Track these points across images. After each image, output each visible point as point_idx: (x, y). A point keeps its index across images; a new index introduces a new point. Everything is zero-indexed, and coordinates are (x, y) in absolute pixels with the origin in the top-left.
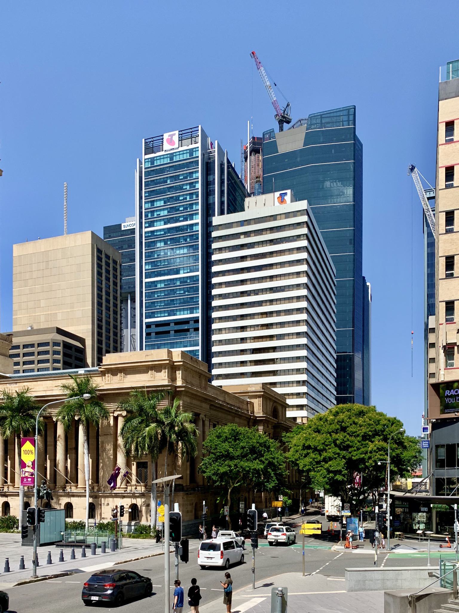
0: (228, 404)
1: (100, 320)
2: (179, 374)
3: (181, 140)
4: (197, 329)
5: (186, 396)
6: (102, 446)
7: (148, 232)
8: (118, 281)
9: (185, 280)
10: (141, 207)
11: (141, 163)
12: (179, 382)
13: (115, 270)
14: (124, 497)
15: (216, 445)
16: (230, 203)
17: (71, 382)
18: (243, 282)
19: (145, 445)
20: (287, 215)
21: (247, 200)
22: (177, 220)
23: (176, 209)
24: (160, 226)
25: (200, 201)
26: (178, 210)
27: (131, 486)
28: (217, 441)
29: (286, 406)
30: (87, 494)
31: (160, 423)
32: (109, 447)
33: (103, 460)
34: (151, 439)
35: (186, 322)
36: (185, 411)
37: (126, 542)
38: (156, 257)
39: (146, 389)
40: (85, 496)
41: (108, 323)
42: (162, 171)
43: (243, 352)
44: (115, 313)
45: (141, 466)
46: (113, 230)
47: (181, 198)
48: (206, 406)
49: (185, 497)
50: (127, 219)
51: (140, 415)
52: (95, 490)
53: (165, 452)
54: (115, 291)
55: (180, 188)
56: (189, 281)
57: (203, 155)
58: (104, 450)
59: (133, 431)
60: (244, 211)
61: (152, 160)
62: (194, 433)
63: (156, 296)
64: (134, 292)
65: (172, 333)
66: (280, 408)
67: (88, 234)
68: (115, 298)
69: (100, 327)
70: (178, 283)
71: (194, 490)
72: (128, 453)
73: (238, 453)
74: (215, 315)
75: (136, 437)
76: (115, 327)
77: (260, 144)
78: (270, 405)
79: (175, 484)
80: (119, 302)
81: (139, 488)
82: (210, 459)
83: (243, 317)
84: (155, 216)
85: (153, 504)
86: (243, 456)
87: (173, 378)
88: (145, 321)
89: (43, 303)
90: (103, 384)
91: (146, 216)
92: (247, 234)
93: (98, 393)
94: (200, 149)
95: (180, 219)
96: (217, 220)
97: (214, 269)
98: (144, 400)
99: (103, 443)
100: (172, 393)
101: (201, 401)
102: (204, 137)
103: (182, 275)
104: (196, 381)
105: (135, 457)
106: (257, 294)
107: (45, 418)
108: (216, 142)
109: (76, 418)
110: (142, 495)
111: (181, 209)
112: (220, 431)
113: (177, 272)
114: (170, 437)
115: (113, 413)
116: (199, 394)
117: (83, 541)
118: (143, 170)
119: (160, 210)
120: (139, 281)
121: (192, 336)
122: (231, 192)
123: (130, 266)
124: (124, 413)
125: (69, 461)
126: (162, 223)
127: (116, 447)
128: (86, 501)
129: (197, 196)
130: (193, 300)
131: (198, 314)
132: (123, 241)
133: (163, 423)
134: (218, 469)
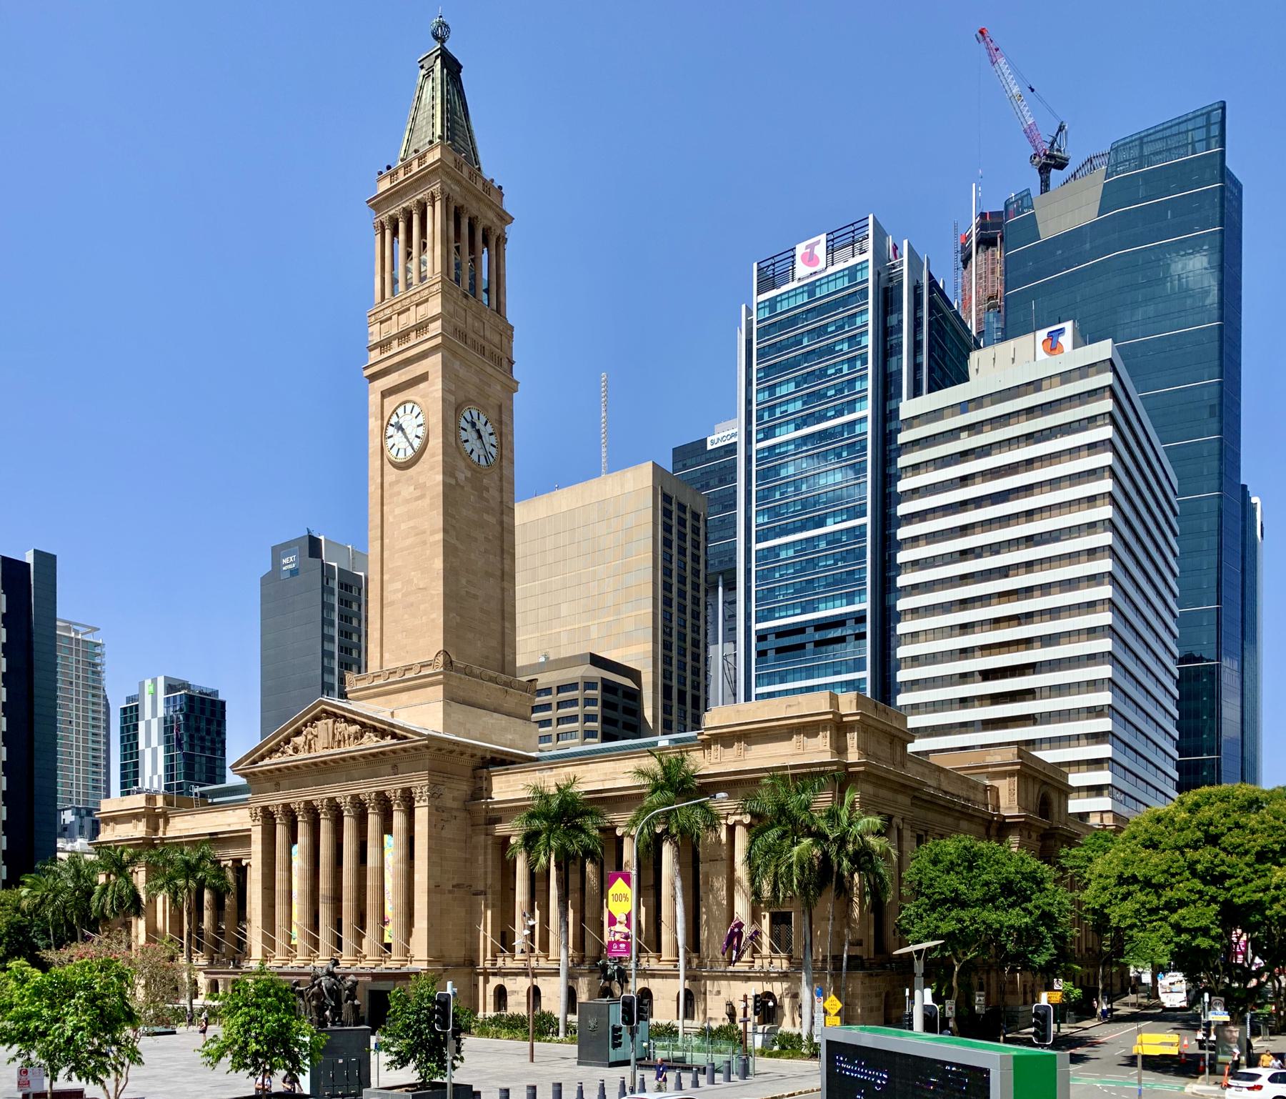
0: (946, 793)
1: (667, 632)
2: (852, 740)
3: (831, 250)
4: (863, 636)
5: (867, 781)
6: (707, 882)
7: (763, 450)
8: (702, 552)
9: (838, 536)
10: (749, 402)
11: (749, 312)
12: (853, 756)
13: (696, 531)
14: (748, 979)
15: (931, 879)
16: (933, 365)
17: (651, 764)
18: (964, 530)
19: (792, 881)
20: (1065, 377)
21: (974, 356)
22: (822, 418)
23: (820, 395)
24: (787, 434)
25: (870, 371)
26: (825, 396)
27: (761, 958)
28: (932, 872)
29: (1067, 791)
30: (682, 973)
31: (819, 837)
32: (720, 884)
33: (708, 907)
34: (802, 868)
35: (838, 622)
36: (866, 813)
37: (761, 1064)
38: (778, 497)
39: (789, 772)
40: (677, 977)
41: (682, 637)
42: (792, 321)
43: (964, 677)
44: (696, 615)
45: (780, 920)
46: (690, 453)
47: (831, 371)
48: (904, 800)
49: (867, 981)
50: (717, 427)
51: (779, 822)
52: (694, 966)
53: (830, 893)
54: (696, 573)
55: (830, 350)
56: (844, 538)
57: (877, 274)
58: (711, 889)
59: (766, 853)
60: (967, 380)
61: (773, 303)
62: (886, 855)
63: (777, 575)
64: (733, 571)
65: (810, 647)
66: (1054, 797)
67: (647, 468)
68: (696, 587)
69: (667, 646)
70: (823, 545)
71: (885, 968)
72: (757, 893)
73: (978, 894)
74: (902, 604)
75: (773, 864)
76: (696, 643)
77: (999, 226)
78: (1034, 791)
79: (848, 957)
80: (702, 594)
81: (776, 962)
82: (918, 907)
83: (964, 604)
84: (778, 415)
85: (805, 994)
86: (983, 902)
87: (840, 749)
88: (755, 627)
89: (564, 609)
90: (707, 764)
91: (760, 418)
92: (973, 428)
93: (697, 781)
94: (871, 264)
95: (829, 414)
96: (908, 407)
97: (903, 509)
98: (788, 792)
99: (707, 876)
100: (841, 778)
101: (895, 791)
102: (880, 234)
103: (830, 528)
104: (884, 751)
105: (769, 904)
106: (998, 553)
107: (602, 830)
108: (905, 242)
109: (658, 830)
110: (783, 976)
111: (831, 392)
112: (938, 850)
113: (820, 523)
114: (840, 865)
115: (726, 819)
116: (892, 777)
117: (682, 1060)
118: (755, 326)
119: (787, 402)
120: (744, 549)
121: (847, 652)
122: (937, 341)
123: (722, 520)
124: (747, 819)
125: (643, 909)
126: (792, 426)
127: (731, 883)
128: (680, 985)
129: (865, 362)
130: (854, 576)
131: (865, 605)
132: (705, 473)
133: (826, 838)
134: (937, 927)
